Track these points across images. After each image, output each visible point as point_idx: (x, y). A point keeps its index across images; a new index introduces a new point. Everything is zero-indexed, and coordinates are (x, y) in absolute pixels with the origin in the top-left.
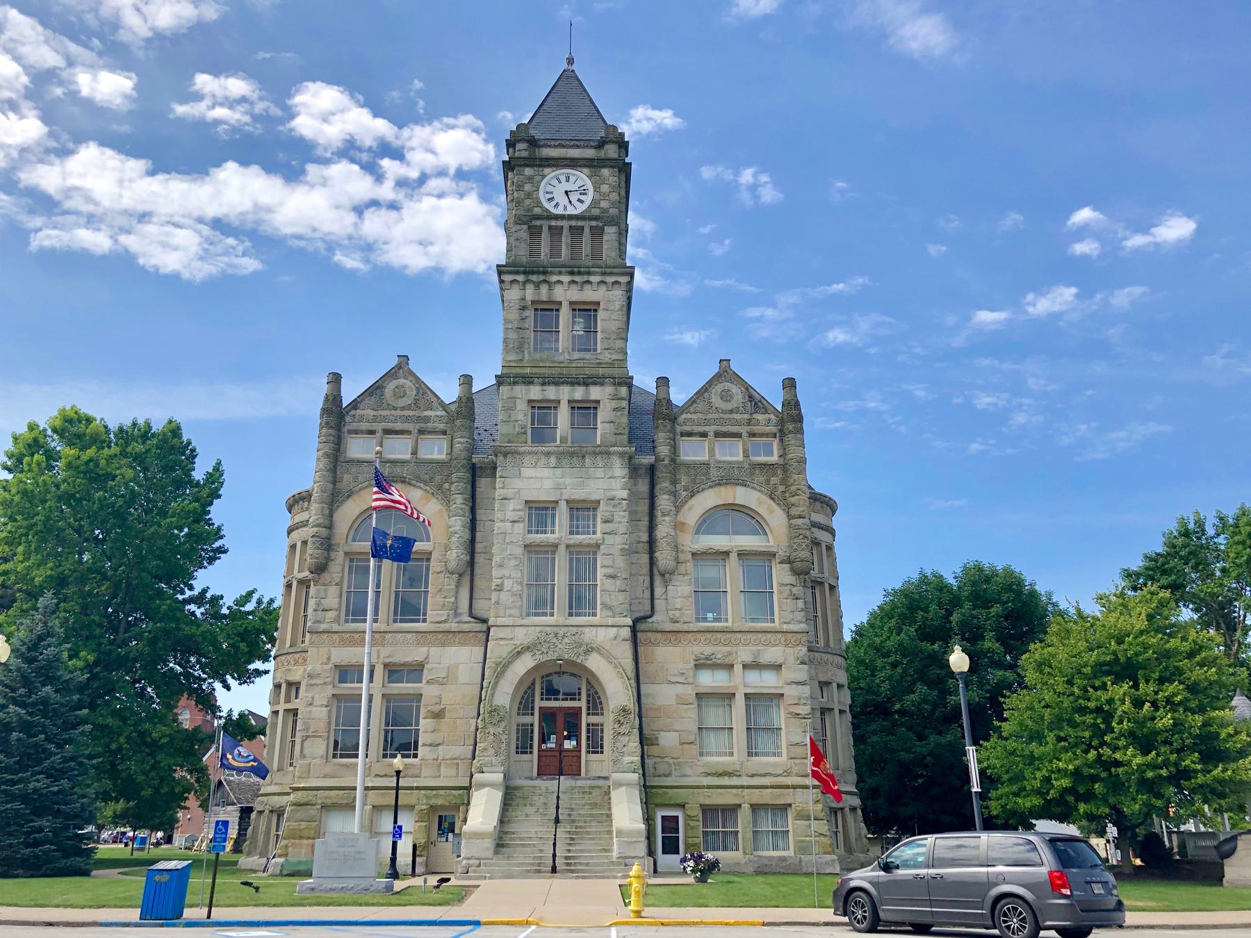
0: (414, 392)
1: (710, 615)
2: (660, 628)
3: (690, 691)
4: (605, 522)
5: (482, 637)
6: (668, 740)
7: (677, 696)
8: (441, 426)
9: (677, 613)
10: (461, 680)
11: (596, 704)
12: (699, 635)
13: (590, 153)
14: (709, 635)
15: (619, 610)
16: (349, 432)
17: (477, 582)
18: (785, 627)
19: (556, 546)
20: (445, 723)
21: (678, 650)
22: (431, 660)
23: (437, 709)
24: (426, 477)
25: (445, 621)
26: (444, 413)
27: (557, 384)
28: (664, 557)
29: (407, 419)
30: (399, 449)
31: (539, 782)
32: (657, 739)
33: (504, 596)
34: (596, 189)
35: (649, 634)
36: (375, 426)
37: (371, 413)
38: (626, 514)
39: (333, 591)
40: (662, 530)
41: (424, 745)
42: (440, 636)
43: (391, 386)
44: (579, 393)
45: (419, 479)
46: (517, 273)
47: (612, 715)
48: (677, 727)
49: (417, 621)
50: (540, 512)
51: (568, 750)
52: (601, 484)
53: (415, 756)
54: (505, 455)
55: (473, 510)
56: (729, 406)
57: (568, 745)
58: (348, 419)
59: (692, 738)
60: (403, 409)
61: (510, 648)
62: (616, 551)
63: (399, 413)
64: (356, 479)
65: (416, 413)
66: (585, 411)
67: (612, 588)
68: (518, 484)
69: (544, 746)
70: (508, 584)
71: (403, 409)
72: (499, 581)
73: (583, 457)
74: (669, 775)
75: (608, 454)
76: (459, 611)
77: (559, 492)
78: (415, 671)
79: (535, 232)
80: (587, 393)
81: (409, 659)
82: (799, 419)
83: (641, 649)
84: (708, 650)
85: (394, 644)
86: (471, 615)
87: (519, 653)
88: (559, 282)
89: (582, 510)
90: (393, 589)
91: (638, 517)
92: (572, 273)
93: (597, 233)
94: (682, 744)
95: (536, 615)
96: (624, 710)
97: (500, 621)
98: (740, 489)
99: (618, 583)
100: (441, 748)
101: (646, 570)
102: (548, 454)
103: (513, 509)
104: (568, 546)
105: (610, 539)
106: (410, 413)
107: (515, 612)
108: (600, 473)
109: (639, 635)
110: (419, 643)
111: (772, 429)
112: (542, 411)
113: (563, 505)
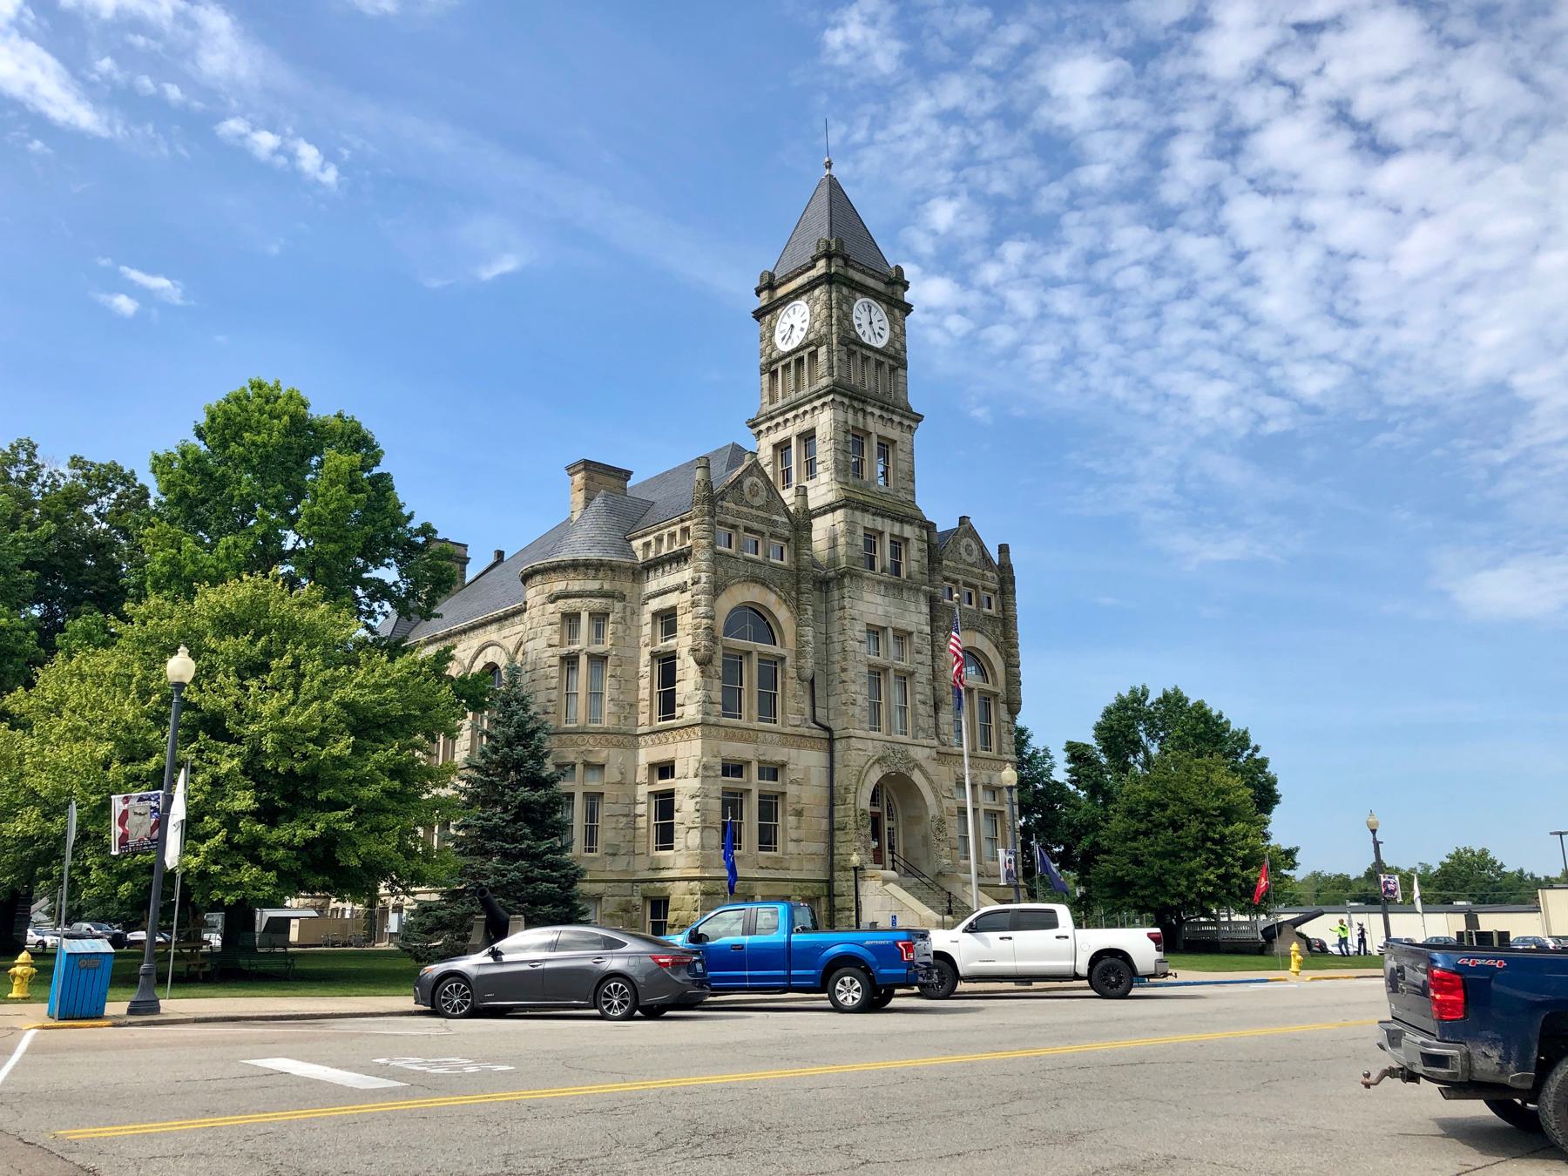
5: (826, 744)
13: (880, 287)
18: (1007, 757)
23: (798, 807)
27: (883, 516)
34: (892, 329)
36: (739, 522)
39: (718, 684)
43: (747, 482)
44: (897, 529)
46: (844, 395)
50: (875, 632)
52: (914, 618)
56: (970, 560)
62: (924, 680)
63: (754, 512)
64: (726, 572)
66: (898, 543)
71: (758, 508)
75: (918, 590)
78: (772, 771)
79: (851, 354)
80: (902, 530)
82: (1013, 582)
86: (815, 722)
88: (872, 414)
92: (882, 408)
93: (893, 369)
102: (879, 582)
103: (858, 630)
107: (867, 726)
111: (994, 586)
112: (872, 537)
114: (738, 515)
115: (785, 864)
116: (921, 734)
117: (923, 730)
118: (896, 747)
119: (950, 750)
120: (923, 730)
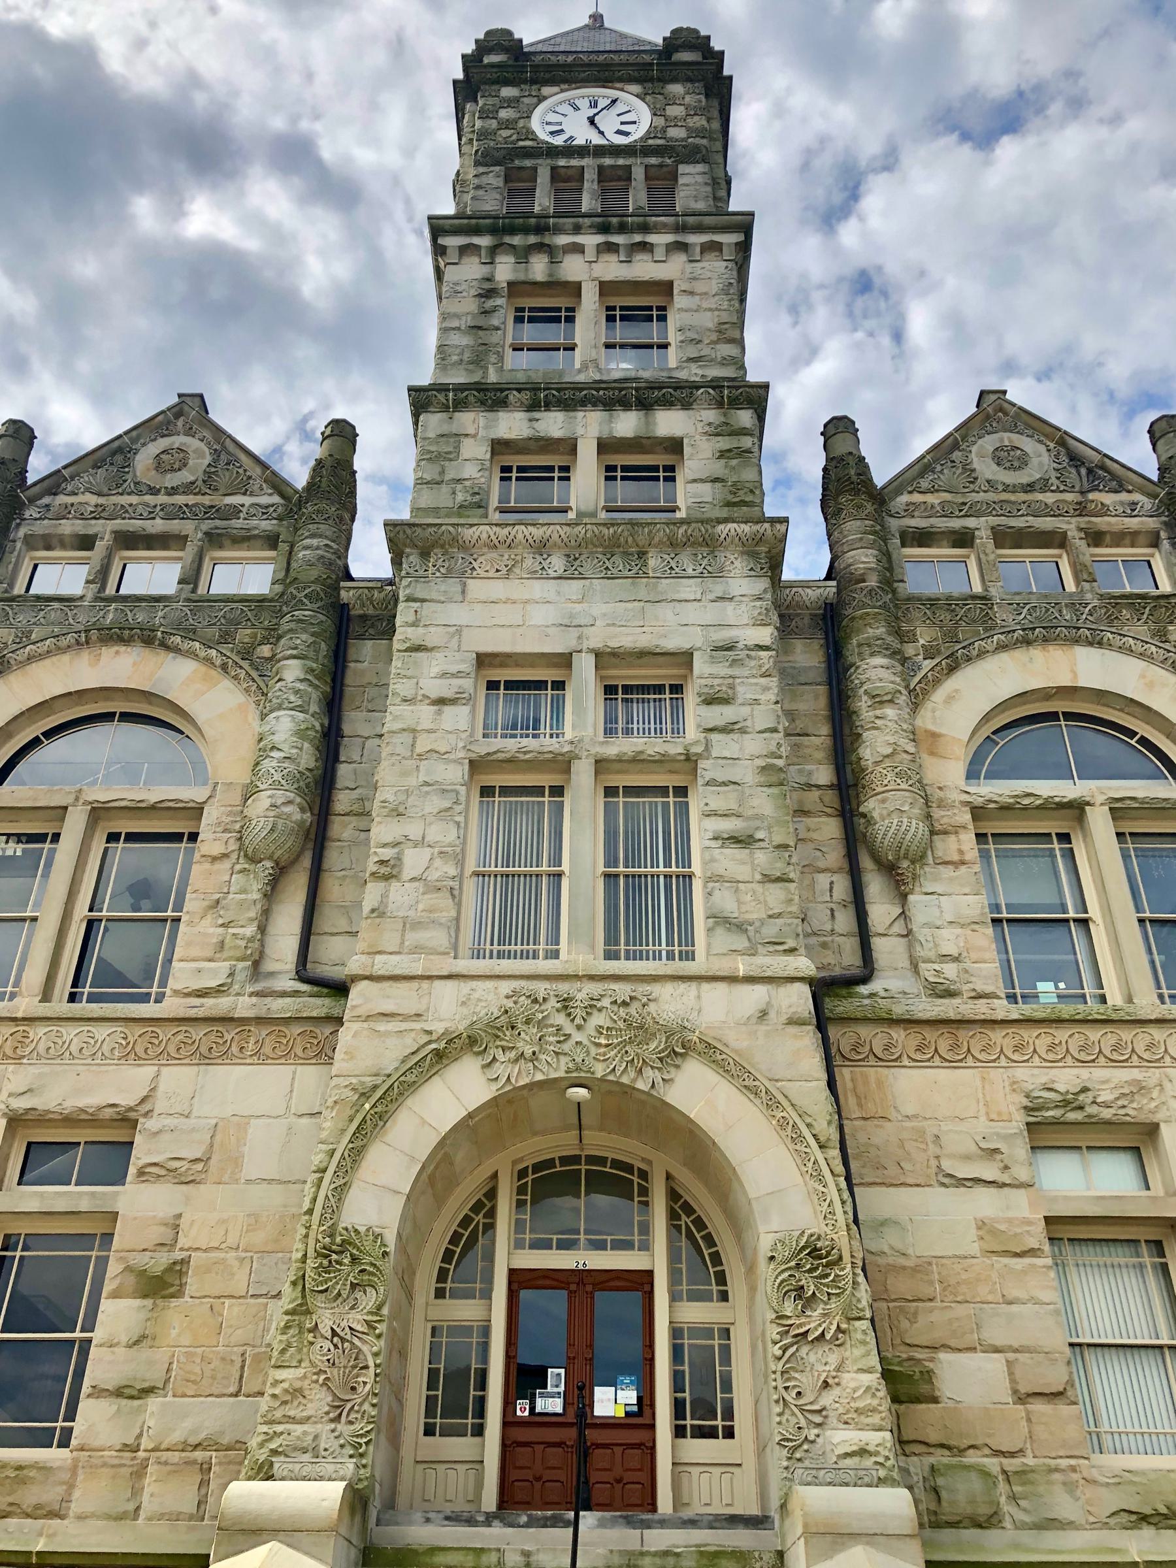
0: (208, 459)
1: (1045, 987)
2: (898, 1010)
3: (1022, 1213)
4: (710, 700)
6: (969, 1382)
7: (981, 1225)
8: (266, 525)
9: (950, 970)
10: (251, 1170)
11: (704, 1256)
12: (1028, 1034)
14: (1062, 1034)
15: (770, 931)
16: (31, 542)
17: (334, 889)
19: (563, 764)
20: (180, 1320)
21: (966, 1077)
22: (160, 1105)
23: (162, 1260)
24: (214, 633)
25: (219, 991)
26: (276, 499)
28: (890, 813)
29: (177, 513)
30: (152, 576)
31: (495, 1535)
32: (928, 1376)
33: (400, 896)
35: (865, 1032)
36: (96, 526)
37: (93, 499)
38: (773, 682)
40: (878, 741)
41: (98, 1392)
42: (198, 1033)
45: (190, 634)
47: (767, 1275)
48: (995, 1334)
49: (144, 998)
51: (609, 1424)
52: (694, 614)
53: (64, 1443)
54: (425, 554)
55: (333, 704)
57: (610, 1402)
58: (31, 512)
59: (1055, 1378)
60: (172, 491)
61: (410, 1043)
62: (746, 773)
63: (162, 499)
65: (206, 500)
67: (742, 872)
68: (457, 614)
69: (522, 1409)
70: (414, 861)
71: (172, 491)
72: (387, 853)
73: (642, 555)
74: (989, 1521)
76: (268, 966)
77: (574, 633)
81: (91, 1100)
83: (844, 1075)
84: (1067, 1079)
85: (59, 1054)
86: (302, 974)
87: (440, 1056)
89: (643, 685)
90: (81, 910)
91: (800, 725)
94: (1022, 1398)
95: (500, 955)
96: (815, 1255)
97: (383, 964)
98: (1083, 654)
99: (761, 857)
100: (153, 1403)
101: (835, 856)
102: (542, 548)
104: (601, 765)
105: (722, 745)
106: (191, 500)
107: (438, 938)
108: (689, 589)
109: (833, 1032)
110: (129, 1055)
113: (585, 666)
114: (99, 513)
115: (30, 1496)
116: (725, 940)
117: (738, 926)
118: (584, 992)
119: (981, 1009)
120: (738, 926)
